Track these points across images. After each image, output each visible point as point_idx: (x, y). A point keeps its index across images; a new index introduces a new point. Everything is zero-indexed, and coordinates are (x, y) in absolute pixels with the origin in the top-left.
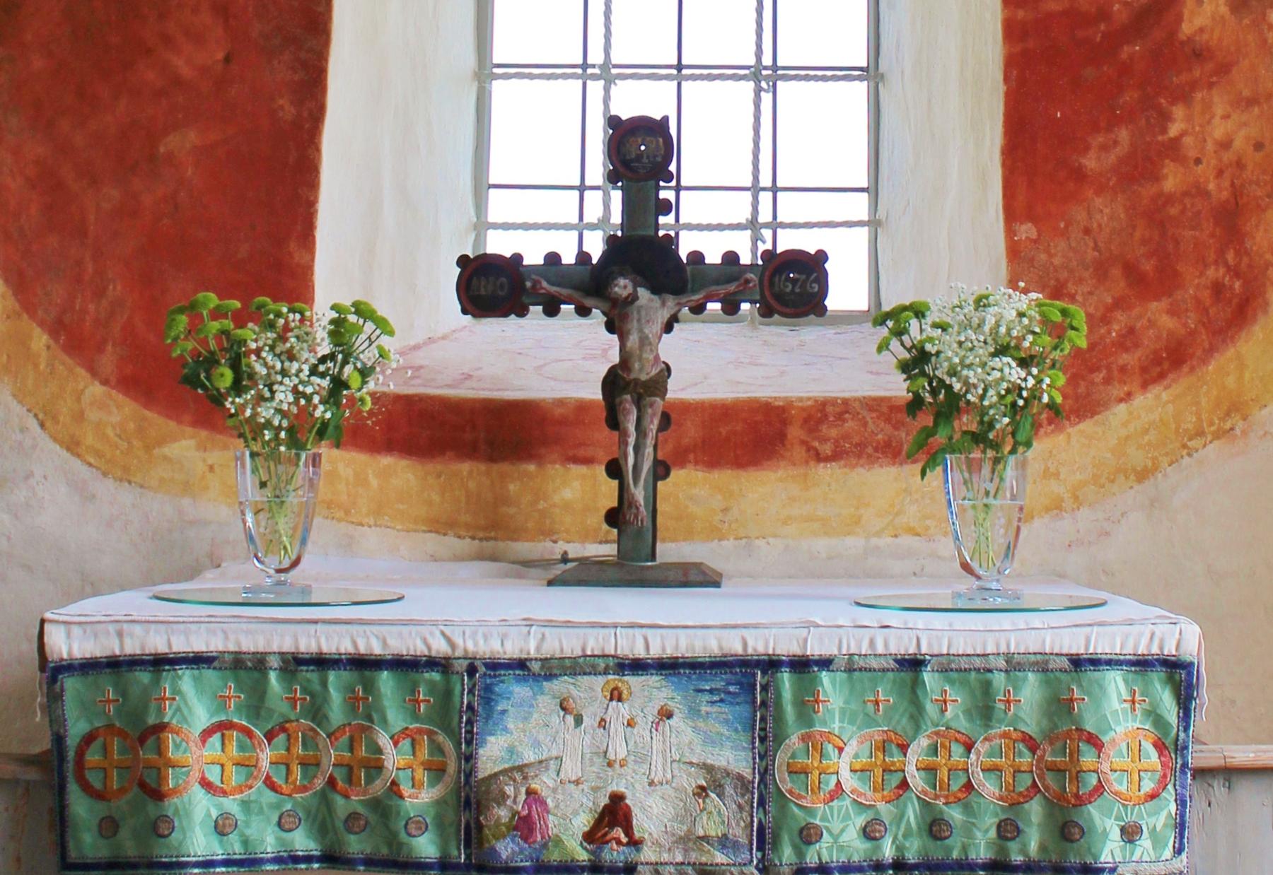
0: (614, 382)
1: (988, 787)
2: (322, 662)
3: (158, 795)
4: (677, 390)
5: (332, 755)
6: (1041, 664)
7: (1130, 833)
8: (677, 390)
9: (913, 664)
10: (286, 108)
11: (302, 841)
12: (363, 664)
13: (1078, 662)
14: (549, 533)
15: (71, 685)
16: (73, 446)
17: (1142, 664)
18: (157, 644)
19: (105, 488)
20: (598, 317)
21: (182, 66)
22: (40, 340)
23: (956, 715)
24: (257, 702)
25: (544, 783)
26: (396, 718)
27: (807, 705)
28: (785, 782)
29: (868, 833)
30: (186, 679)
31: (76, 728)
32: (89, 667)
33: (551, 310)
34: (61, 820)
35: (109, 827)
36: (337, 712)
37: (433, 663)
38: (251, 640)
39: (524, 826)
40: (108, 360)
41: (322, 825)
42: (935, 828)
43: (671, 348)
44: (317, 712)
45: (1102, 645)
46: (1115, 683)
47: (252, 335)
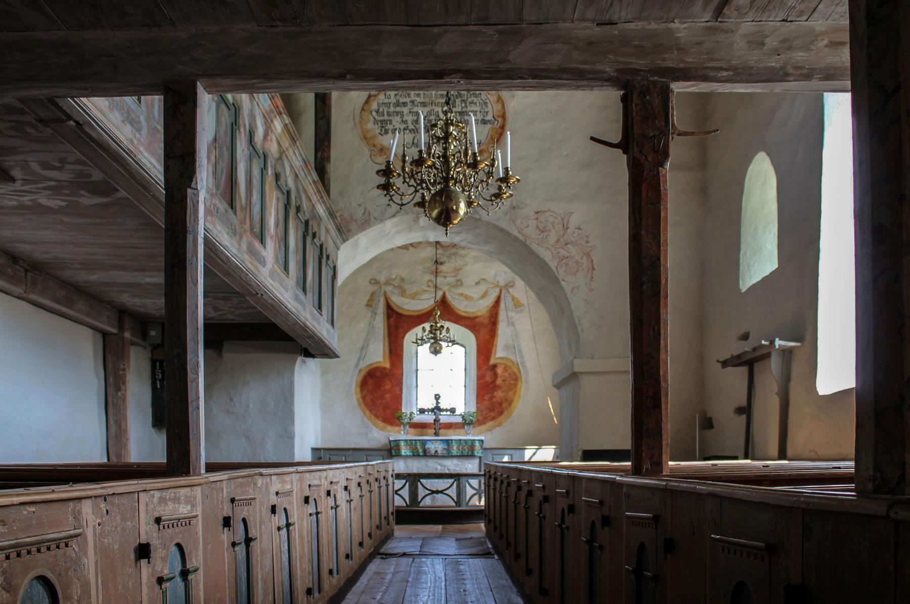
2: (412, 440)
7: (478, 453)
9: (460, 440)
11: (411, 454)
12: (416, 440)
13: (474, 440)
18: (399, 439)
23: (464, 444)
24: (407, 443)
25: (431, 449)
26: (418, 444)
27: (452, 443)
29: (457, 453)
30: (401, 442)
31: (392, 445)
32: (393, 441)
34: (391, 453)
35: (395, 453)
36: (414, 444)
37: (422, 440)
38: (407, 438)
39: (429, 452)
41: (413, 452)
42: (462, 452)
44: (412, 444)
46: (477, 442)
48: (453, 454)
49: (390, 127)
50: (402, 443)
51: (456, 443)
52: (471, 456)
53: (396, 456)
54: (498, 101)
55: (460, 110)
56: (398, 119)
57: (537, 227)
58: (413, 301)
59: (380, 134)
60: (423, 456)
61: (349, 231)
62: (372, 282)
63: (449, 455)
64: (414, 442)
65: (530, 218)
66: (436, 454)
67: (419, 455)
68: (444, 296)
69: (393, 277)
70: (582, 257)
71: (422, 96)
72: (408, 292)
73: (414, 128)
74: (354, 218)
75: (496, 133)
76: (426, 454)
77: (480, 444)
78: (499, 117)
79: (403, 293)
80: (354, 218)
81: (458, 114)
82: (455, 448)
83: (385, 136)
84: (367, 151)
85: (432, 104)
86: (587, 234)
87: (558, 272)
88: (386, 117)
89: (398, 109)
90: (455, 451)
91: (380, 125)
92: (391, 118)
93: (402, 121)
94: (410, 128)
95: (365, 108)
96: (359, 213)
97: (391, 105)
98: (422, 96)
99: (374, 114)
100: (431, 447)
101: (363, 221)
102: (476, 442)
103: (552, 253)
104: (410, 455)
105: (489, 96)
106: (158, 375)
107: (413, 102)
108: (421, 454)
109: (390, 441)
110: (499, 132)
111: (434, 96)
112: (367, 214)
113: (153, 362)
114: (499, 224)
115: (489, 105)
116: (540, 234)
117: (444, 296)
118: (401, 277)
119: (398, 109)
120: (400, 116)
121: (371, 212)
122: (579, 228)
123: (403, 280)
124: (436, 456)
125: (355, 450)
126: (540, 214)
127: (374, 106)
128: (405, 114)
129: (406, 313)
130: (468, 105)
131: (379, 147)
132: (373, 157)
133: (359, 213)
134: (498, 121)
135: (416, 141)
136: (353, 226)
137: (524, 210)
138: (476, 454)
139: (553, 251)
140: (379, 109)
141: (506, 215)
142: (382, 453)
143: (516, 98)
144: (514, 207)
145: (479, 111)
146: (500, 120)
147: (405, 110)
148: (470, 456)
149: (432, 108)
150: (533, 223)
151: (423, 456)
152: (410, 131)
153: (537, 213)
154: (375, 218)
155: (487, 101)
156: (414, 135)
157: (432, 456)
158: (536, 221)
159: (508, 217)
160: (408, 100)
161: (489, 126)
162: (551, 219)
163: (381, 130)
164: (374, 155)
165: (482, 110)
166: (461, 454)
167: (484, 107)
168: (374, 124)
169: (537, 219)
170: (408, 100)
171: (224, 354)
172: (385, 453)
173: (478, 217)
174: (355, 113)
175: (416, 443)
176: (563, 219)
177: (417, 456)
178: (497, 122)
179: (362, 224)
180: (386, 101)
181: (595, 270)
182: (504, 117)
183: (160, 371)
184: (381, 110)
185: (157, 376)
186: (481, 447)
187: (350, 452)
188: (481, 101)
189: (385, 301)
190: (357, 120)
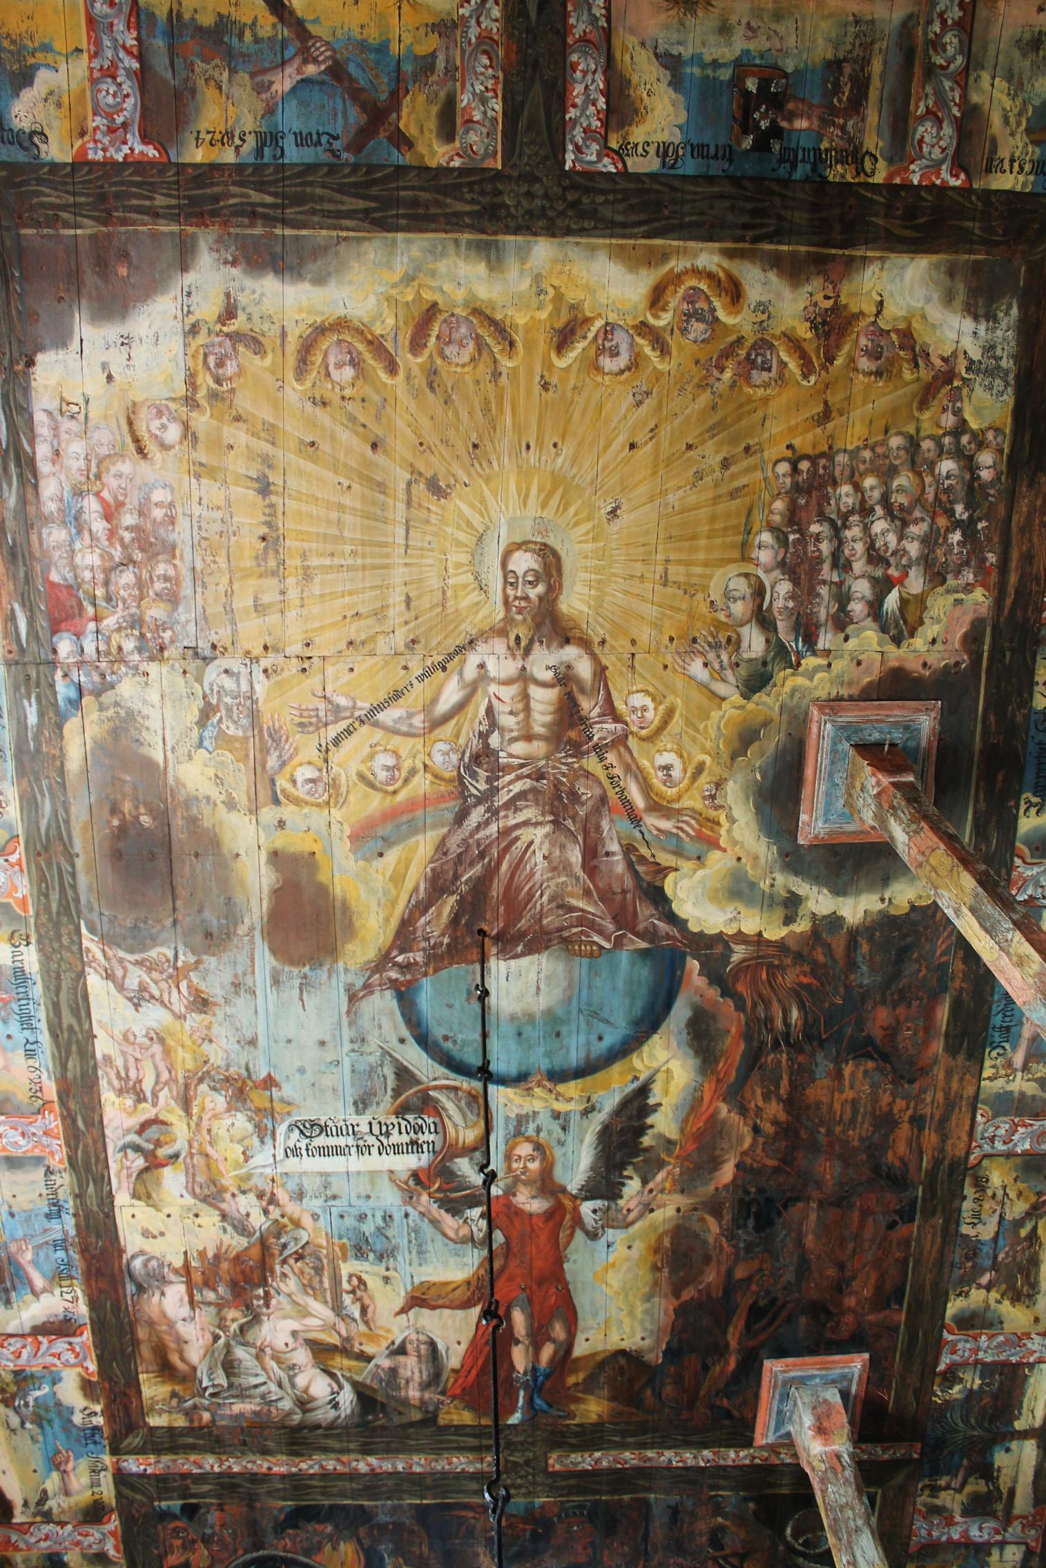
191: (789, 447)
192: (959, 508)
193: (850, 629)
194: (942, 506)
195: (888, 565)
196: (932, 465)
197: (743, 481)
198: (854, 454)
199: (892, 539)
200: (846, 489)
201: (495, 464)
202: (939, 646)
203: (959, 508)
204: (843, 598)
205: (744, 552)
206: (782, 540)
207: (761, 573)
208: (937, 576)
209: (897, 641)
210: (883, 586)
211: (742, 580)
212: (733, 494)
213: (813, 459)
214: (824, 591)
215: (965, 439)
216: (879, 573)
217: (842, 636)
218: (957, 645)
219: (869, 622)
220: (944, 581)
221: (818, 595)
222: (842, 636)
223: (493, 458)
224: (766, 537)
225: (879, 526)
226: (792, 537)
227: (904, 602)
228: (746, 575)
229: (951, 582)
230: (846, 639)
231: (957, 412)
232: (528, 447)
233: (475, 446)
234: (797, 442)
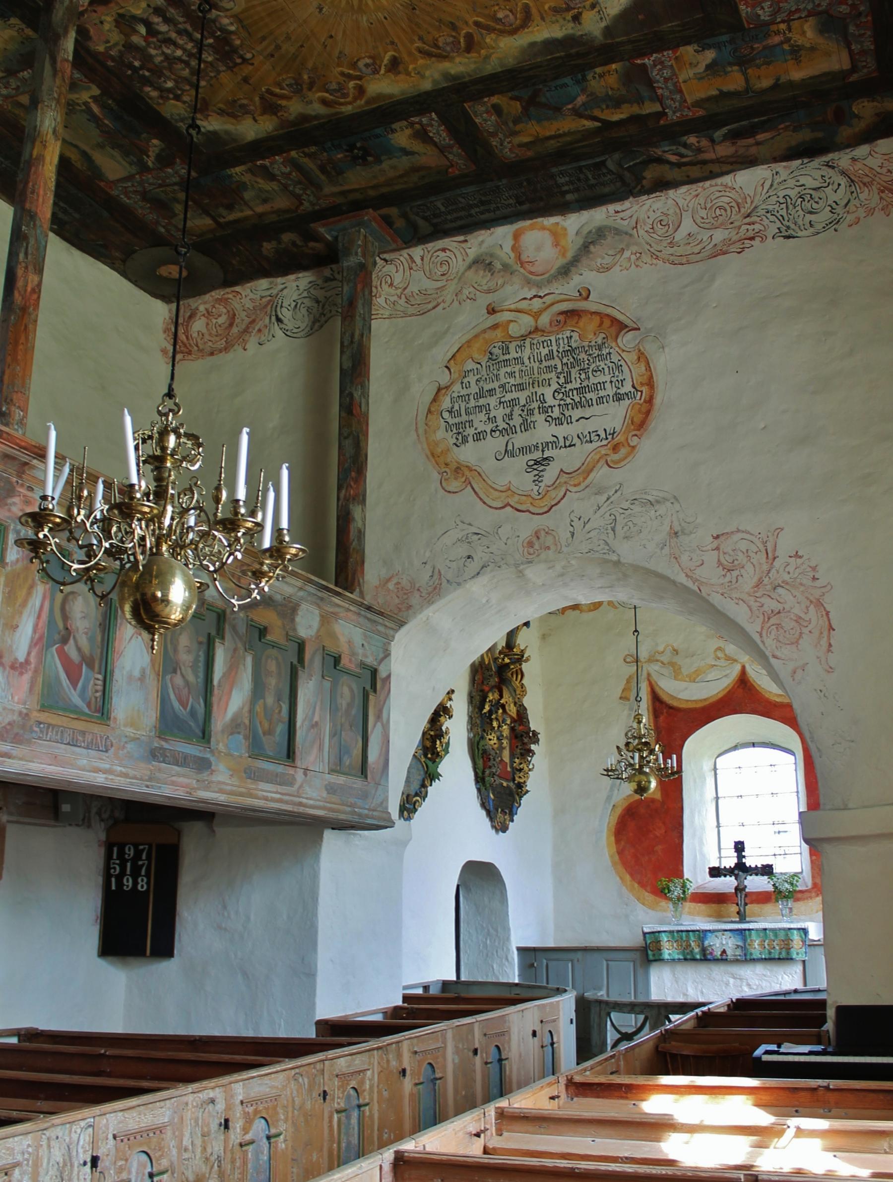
0: (736, 889)
1: (777, 948)
2: (682, 931)
3: (660, 950)
4: (747, 890)
5: (684, 944)
6: (784, 929)
7: (798, 954)
8: (747, 890)
9: (765, 929)
10: (677, 841)
13: (790, 929)
14: (730, 917)
15: (647, 936)
16: (643, 904)
17: (799, 929)
18: (659, 929)
19: (650, 911)
20: (733, 878)
21: (658, 833)
22: (636, 885)
24: (673, 937)
25: (714, 947)
26: (692, 938)
27: (750, 935)
28: (748, 947)
30: (663, 934)
31: (648, 942)
33: (725, 876)
34: (647, 955)
35: (654, 955)
39: (711, 954)
40: (648, 888)
41: (683, 954)
42: (770, 953)
43: (746, 882)
44: (682, 938)
45: (792, 926)
47: (671, 885)
48: (754, 957)
49: (470, 431)
50: (664, 938)
51: (759, 936)
52: (785, 959)
53: (655, 960)
54: (639, 359)
55: (578, 386)
56: (482, 416)
57: (720, 563)
58: (693, 685)
59: (455, 444)
60: (701, 960)
61: (409, 607)
62: (628, 660)
63: (747, 959)
64: (684, 934)
65: (704, 549)
66: (724, 957)
67: (694, 960)
68: (743, 672)
69: (661, 649)
70: (807, 607)
71: (517, 375)
72: (685, 671)
73: (506, 426)
74: (417, 586)
75: (640, 411)
76: (706, 957)
77: (801, 936)
78: (642, 384)
79: (677, 673)
80: (417, 586)
81: (575, 392)
82: (756, 945)
83: (463, 446)
84: (436, 476)
85: (533, 384)
86: (813, 564)
87: (763, 642)
88: (464, 418)
89: (482, 402)
90: (756, 949)
91: (455, 431)
92: (471, 417)
93: (489, 419)
94: (500, 428)
95: (432, 409)
96: (424, 577)
97: (471, 397)
98: (517, 375)
99: (446, 415)
100: (716, 944)
101: (430, 589)
102: (793, 934)
103: (749, 606)
104: (679, 959)
105: (624, 355)
106: (115, 868)
107: (503, 386)
108: (698, 957)
109: (645, 934)
110: (644, 410)
111: (536, 372)
112: (436, 576)
113: (109, 847)
114: (652, 565)
115: (625, 368)
116: (724, 576)
117: (743, 672)
118: (673, 647)
119: (482, 402)
120: (484, 412)
121: (442, 573)
122: (797, 556)
123: (676, 652)
124: (723, 959)
125: (585, 950)
126: (722, 539)
127: (446, 403)
128: (491, 408)
129: (683, 706)
130: (591, 375)
131: (454, 465)
132: (444, 484)
133: (424, 577)
134: (642, 392)
135: (510, 447)
136: (415, 600)
137: (693, 536)
138: (794, 956)
139: (752, 603)
140: (453, 408)
141: (662, 548)
142: (632, 955)
143: (667, 350)
144: (676, 533)
145: (609, 381)
146: (645, 389)
147: (493, 401)
148: (783, 959)
149: (533, 391)
150: (711, 558)
151: (701, 960)
152: (501, 432)
153: (717, 537)
154: (448, 581)
155: (622, 362)
156: (507, 437)
157: (716, 960)
158: (716, 552)
159: (666, 550)
160: (496, 385)
161: (627, 402)
162: (743, 546)
163: (457, 439)
164: (446, 480)
165: (614, 379)
166: (767, 957)
167: (617, 373)
168: (447, 431)
169: (717, 549)
170: (496, 385)
171: (215, 829)
172: (637, 955)
173: (614, 558)
174: (419, 419)
175: (688, 937)
176: (764, 543)
177: (691, 960)
178: (639, 393)
179: (429, 594)
180: (464, 392)
181: (834, 630)
182: (650, 383)
183: (118, 862)
184: (456, 407)
185: (112, 871)
186: (804, 942)
187: (579, 955)
188: (611, 365)
189: (649, 689)
190: (421, 431)
191: (253, 64)
192: (147, 74)
193: (151, 11)
194: (157, 72)
195: (158, 41)
196: (176, 81)
197: (265, 44)
198: (219, 72)
199: (168, 51)
200: (210, 59)
201: (399, 6)
202: (97, 21)
203: (147, 74)
204: (167, 20)
205: (238, 18)
206: (223, 30)
207: (221, 14)
208: (130, 47)
209: (121, 16)
210: (152, 31)
211: (228, 7)
212: (264, 38)
213: (236, 65)
214: (181, 20)
215: (171, 96)
216: (160, 37)
217: (152, 6)
218: (88, 26)
219: (145, 16)
220: (123, 46)
221: (182, 17)
222: (152, 6)
223: (401, 8)
224: (233, 28)
225: (179, 53)
226: (219, 33)
227: (135, 31)
228: (228, 10)
229: (120, 47)
230: (149, 6)
231: (184, 102)
232: (385, 18)
233: (414, 9)
234: (251, 67)
